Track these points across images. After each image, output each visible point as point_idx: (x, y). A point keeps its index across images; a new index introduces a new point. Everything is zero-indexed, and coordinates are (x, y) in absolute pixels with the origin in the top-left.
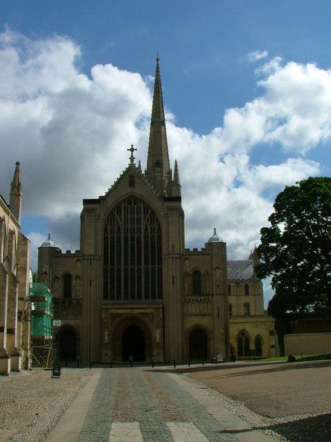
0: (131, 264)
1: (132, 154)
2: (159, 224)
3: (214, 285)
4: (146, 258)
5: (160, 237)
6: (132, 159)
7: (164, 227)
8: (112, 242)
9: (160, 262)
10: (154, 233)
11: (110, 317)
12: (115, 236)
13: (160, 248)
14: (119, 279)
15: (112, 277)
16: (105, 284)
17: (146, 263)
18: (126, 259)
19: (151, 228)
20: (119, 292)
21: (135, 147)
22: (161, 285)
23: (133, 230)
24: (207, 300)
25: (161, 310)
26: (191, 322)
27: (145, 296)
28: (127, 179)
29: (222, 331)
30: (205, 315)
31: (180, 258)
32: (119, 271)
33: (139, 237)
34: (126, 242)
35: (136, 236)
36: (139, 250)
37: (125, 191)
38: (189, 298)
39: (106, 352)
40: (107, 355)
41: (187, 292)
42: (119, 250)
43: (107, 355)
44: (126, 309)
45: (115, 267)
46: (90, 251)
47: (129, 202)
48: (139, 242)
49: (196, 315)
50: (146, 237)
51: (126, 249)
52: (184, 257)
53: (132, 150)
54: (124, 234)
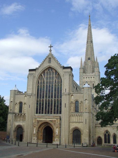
0: (48, 98)
1: (51, 48)
2: (61, 79)
3: (84, 108)
4: (55, 96)
5: (61, 85)
6: (50, 50)
7: (62, 80)
8: (41, 88)
9: (61, 97)
10: (59, 83)
11: (36, 122)
12: (42, 85)
13: (61, 90)
14: (43, 105)
15: (40, 104)
16: (37, 107)
17: (55, 97)
18: (46, 96)
19: (58, 81)
20: (43, 110)
21: (52, 46)
22: (61, 108)
23: (50, 82)
24: (81, 115)
25: (59, 119)
26: (73, 126)
27: (54, 112)
28: (48, 60)
29: (88, 131)
30: (80, 122)
31: (68, 95)
32: (43, 101)
33: (52, 85)
34: (47, 88)
35: (51, 85)
36: (52, 91)
37: (46, 65)
38: (73, 114)
39: (34, 138)
40: (34, 139)
41: (72, 111)
42: (44, 92)
43: (34, 139)
44: (44, 118)
45: (42, 99)
46: (30, 92)
47: (49, 70)
48: (52, 88)
49: (76, 122)
50: (55, 85)
51: (46, 91)
52: (72, 94)
53: (51, 47)
54: (46, 84)
